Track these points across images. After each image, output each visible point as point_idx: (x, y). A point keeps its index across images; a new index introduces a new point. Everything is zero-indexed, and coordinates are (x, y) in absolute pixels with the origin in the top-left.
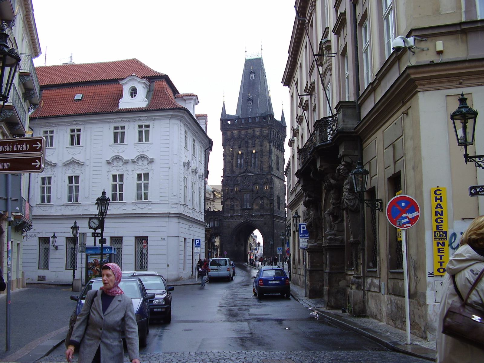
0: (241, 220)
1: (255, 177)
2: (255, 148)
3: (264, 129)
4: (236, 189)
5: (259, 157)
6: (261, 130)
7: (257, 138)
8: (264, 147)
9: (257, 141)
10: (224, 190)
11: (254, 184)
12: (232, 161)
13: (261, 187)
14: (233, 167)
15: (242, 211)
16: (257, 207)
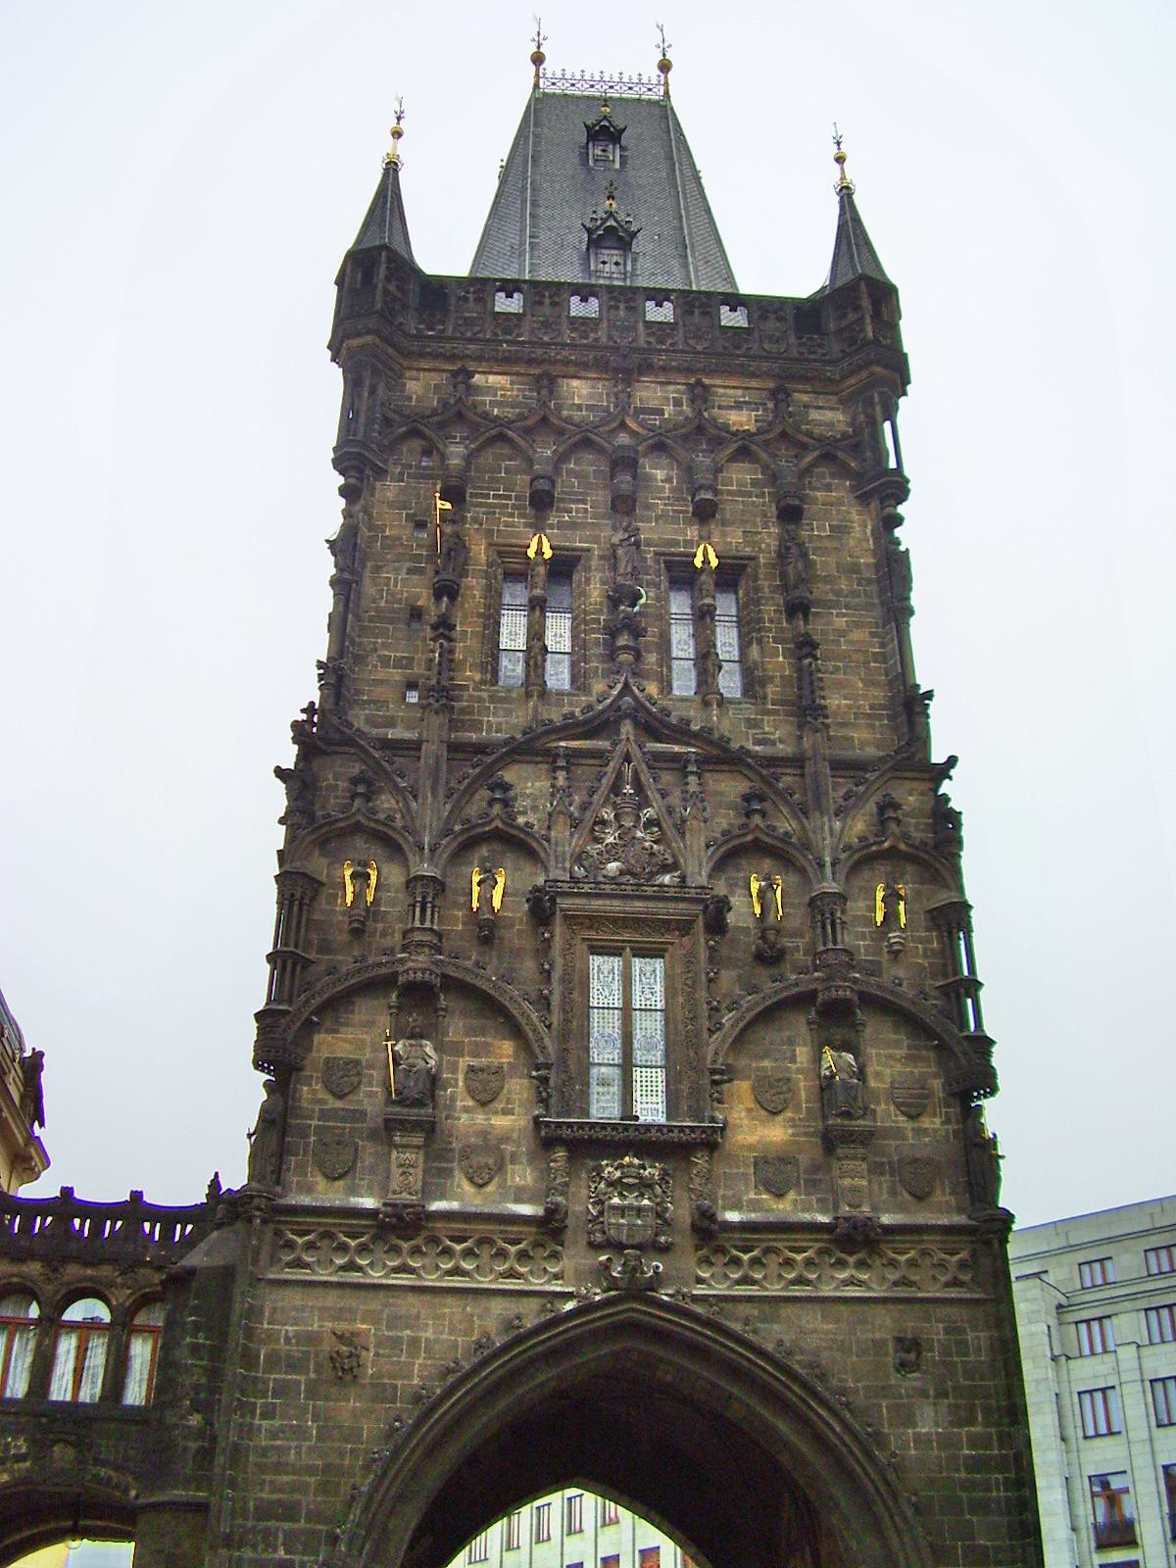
0: (537, 1284)
1: (730, 787)
2: (714, 527)
3: (805, 398)
4: (488, 882)
5: (769, 610)
6: (780, 395)
7: (743, 453)
8: (815, 530)
9: (740, 475)
10: (321, 884)
11: (732, 855)
12: (433, 610)
13: (831, 886)
14: (448, 662)
15: (561, 1154)
16: (776, 1133)
